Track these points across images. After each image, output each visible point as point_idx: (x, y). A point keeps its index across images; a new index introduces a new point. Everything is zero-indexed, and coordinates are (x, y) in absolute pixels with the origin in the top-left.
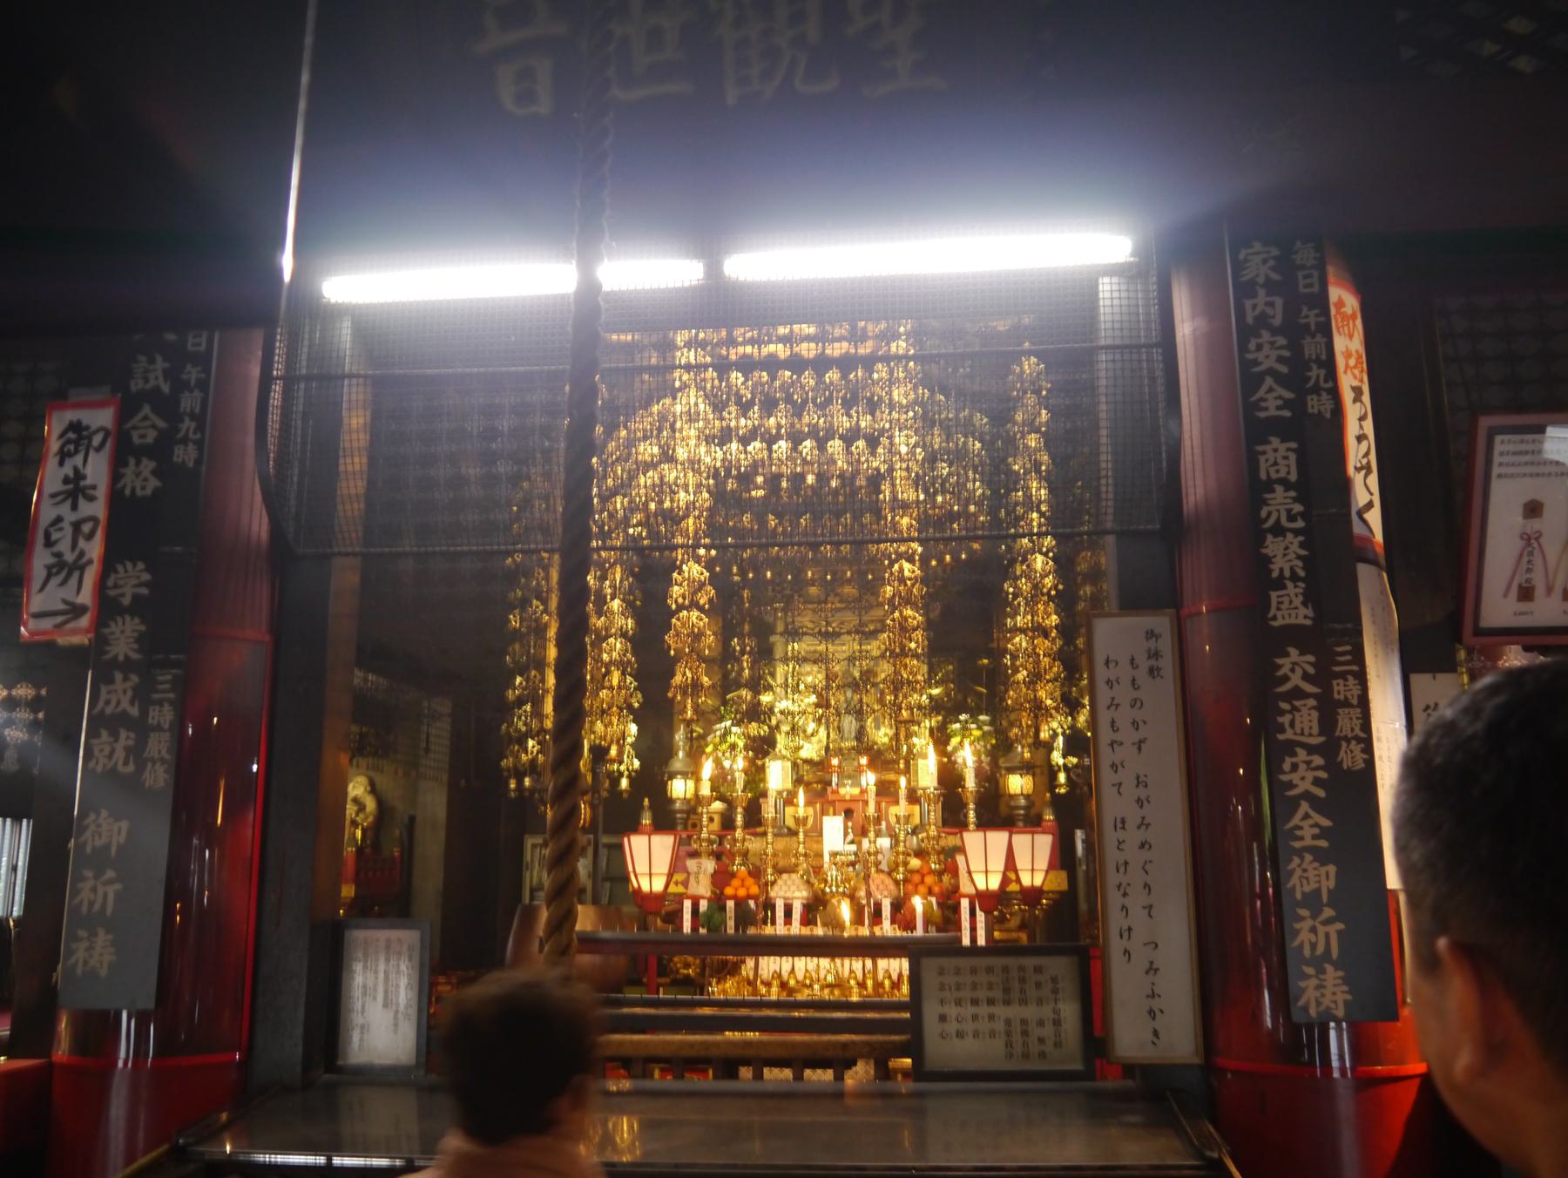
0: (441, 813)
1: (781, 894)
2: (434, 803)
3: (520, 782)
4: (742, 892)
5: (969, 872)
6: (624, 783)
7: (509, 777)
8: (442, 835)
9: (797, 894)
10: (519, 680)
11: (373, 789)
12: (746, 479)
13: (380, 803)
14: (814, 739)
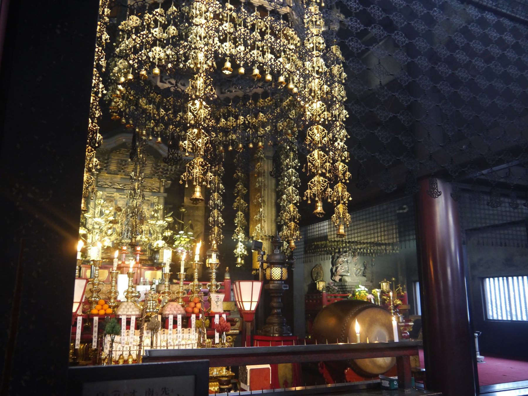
1: (125, 313)
4: (102, 312)
5: (242, 302)
9: (134, 313)
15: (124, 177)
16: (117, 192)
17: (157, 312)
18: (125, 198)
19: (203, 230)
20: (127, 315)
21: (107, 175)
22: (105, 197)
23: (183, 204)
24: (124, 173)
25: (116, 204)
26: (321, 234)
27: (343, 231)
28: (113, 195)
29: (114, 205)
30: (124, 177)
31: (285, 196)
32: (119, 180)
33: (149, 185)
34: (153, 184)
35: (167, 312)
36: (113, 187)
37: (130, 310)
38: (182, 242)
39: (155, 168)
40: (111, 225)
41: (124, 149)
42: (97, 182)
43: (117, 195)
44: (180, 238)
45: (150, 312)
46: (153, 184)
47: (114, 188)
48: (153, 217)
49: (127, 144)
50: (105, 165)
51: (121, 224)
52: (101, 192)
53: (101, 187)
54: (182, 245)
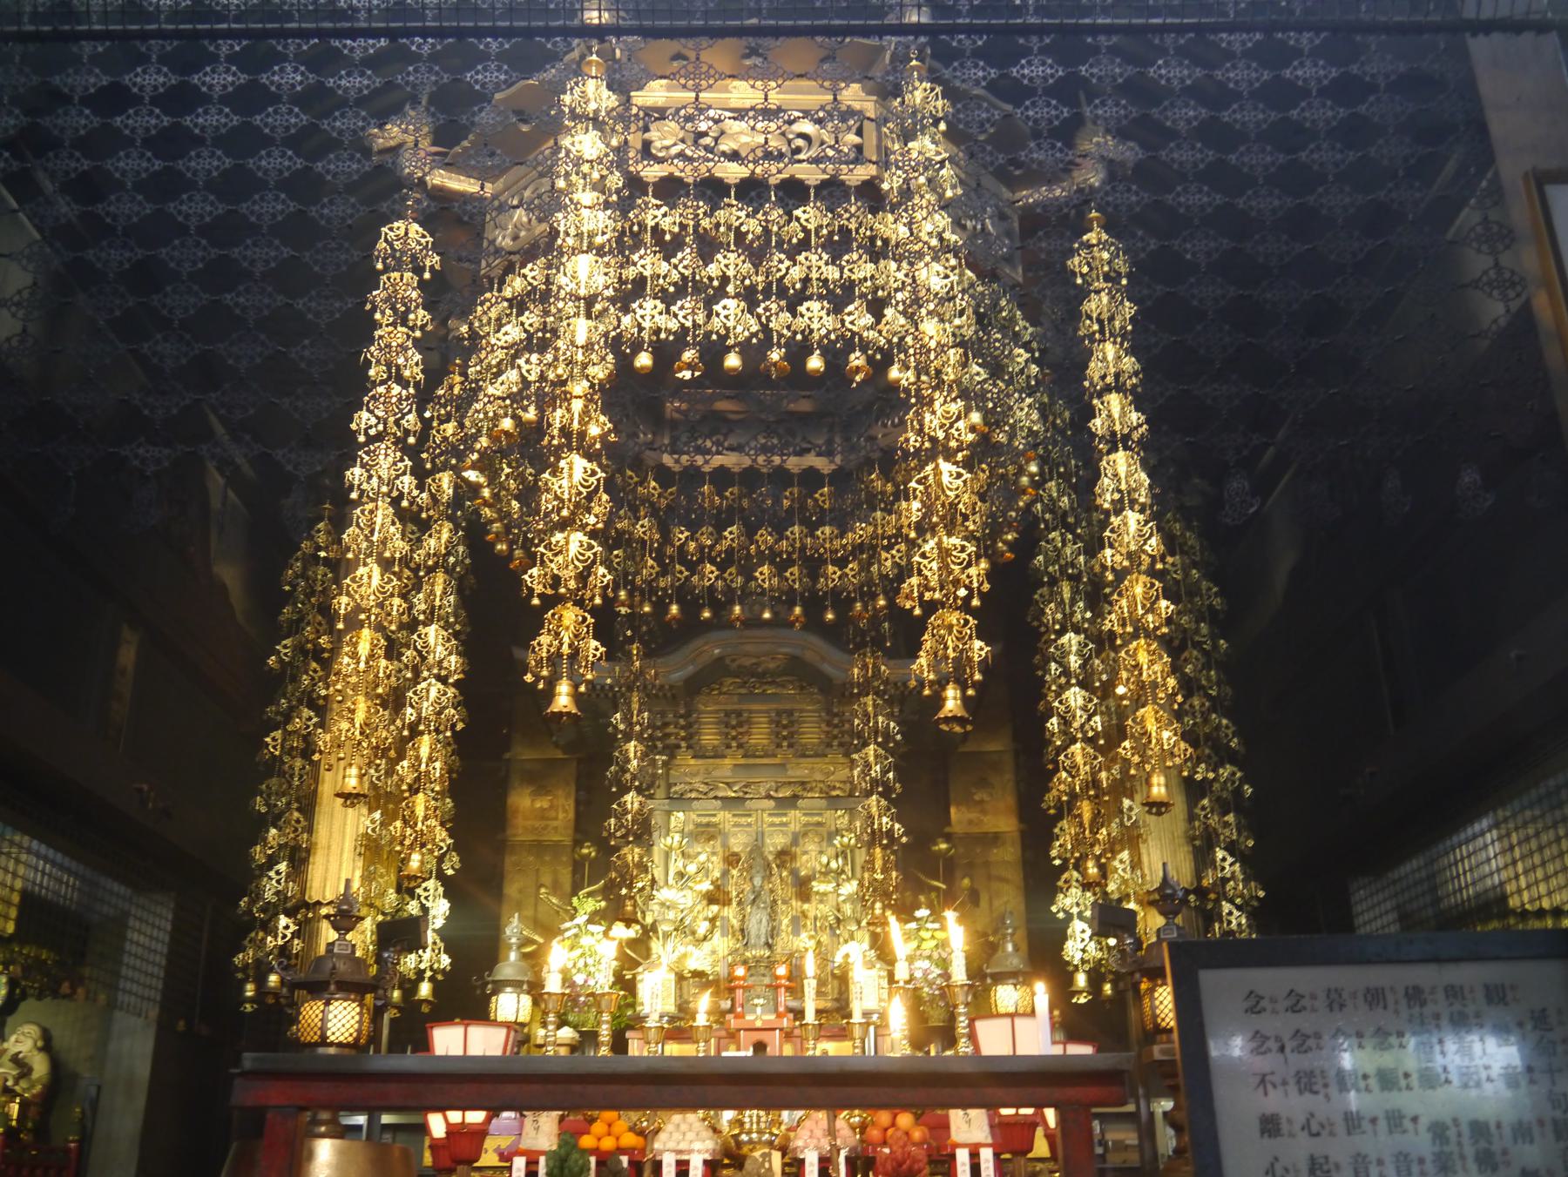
0: (143, 1070)
1: (671, 1145)
2: (135, 1048)
3: (261, 981)
4: (608, 1144)
6: (425, 990)
7: (246, 980)
8: (140, 1101)
10: (273, 831)
11: (47, 1044)
12: (666, 351)
13: (56, 1065)
14: (707, 946)
15: (743, 761)
16: (723, 808)
17: (770, 1144)
18: (749, 825)
19: (1022, 907)
20: (680, 1152)
21: (692, 762)
22: (691, 827)
23: (947, 830)
24: (741, 751)
25: (725, 845)
26: (1486, 891)
27: (1163, 790)
28: (713, 820)
29: (719, 849)
30: (743, 761)
31: (1054, 720)
32: (729, 774)
33: (819, 777)
34: (828, 774)
35: (800, 1143)
36: (711, 794)
37: (690, 1136)
38: (925, 945)
39: (829, 724)
40: (715, 908)
41: (730, 680)
42: (669, 786)
43: (724, 817)
44: (919, 930)
45: (751, 1141)
46: (828, 774)
47: (716, 798)
48: (826, 872)
49: (728, 661)
50: (683, 734)
51: (740, 903)
52: (681, 815)
53: (680, 801)
54: (927, 953)
